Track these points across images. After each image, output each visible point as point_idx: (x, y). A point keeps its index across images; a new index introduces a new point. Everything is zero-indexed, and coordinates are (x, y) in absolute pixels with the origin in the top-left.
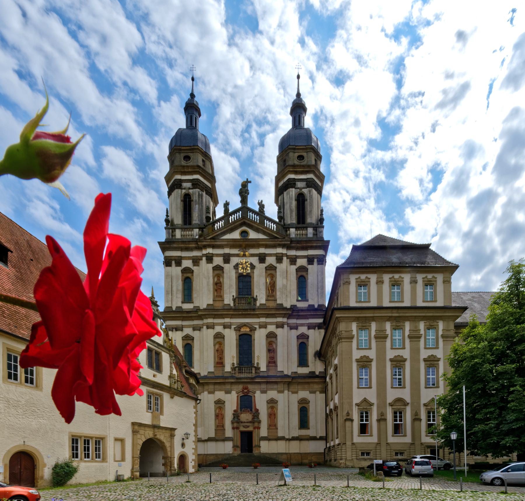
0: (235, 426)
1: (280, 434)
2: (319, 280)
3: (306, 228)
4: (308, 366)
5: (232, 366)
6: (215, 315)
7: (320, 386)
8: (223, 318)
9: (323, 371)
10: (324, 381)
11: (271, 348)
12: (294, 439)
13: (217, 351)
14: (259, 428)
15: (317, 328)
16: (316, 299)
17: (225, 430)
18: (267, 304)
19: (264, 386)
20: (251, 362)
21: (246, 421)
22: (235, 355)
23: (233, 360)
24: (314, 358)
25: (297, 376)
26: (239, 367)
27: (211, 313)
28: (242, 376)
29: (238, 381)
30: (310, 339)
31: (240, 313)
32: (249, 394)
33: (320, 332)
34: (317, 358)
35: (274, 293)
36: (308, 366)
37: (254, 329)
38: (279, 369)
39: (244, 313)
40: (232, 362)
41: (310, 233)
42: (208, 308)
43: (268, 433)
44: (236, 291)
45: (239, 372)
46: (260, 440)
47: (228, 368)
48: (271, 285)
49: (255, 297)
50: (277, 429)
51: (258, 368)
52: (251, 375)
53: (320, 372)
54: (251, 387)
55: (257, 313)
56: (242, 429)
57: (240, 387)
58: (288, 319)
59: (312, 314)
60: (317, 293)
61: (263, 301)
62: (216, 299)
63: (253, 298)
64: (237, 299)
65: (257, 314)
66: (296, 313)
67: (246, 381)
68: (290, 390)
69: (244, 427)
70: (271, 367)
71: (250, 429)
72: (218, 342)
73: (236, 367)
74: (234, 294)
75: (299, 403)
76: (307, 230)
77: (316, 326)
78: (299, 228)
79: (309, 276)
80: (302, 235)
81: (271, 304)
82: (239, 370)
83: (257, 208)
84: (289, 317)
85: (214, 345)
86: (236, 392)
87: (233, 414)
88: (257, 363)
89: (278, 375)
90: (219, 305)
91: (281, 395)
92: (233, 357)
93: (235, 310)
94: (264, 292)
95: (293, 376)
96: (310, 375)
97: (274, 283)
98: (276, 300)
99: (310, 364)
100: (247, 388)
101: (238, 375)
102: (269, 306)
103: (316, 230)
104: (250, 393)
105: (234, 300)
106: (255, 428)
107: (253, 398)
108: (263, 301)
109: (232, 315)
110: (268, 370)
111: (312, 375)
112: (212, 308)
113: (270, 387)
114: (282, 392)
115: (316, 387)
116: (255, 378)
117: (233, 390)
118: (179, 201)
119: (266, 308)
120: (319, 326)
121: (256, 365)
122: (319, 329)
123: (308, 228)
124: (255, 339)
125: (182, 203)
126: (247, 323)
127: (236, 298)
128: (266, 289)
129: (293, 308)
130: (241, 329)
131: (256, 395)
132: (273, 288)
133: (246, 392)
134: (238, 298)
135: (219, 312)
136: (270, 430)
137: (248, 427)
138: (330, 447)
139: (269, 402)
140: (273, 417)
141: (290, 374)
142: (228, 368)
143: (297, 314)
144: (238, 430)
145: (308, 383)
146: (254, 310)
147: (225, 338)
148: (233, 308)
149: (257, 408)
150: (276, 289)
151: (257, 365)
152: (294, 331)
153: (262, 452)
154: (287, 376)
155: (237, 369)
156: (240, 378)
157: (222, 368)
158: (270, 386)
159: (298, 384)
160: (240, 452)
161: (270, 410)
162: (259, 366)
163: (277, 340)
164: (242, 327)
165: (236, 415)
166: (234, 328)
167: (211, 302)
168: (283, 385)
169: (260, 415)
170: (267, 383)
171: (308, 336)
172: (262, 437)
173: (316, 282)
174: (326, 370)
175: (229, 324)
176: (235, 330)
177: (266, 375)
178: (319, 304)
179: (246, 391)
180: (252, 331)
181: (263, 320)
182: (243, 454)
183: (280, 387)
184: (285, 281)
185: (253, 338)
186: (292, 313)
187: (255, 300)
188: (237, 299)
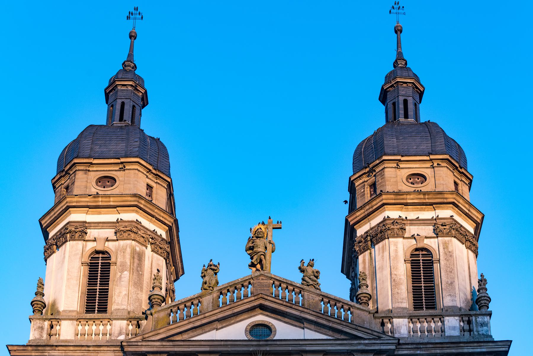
3: (441, 317)
41: (454, 328)
76: (443, 322)
78: (418, 317)
80: (429, 331)
83: (297, 278)
103: (469, 322)
118: (77, 263)
123: (446, 318)
125: (84, 271)
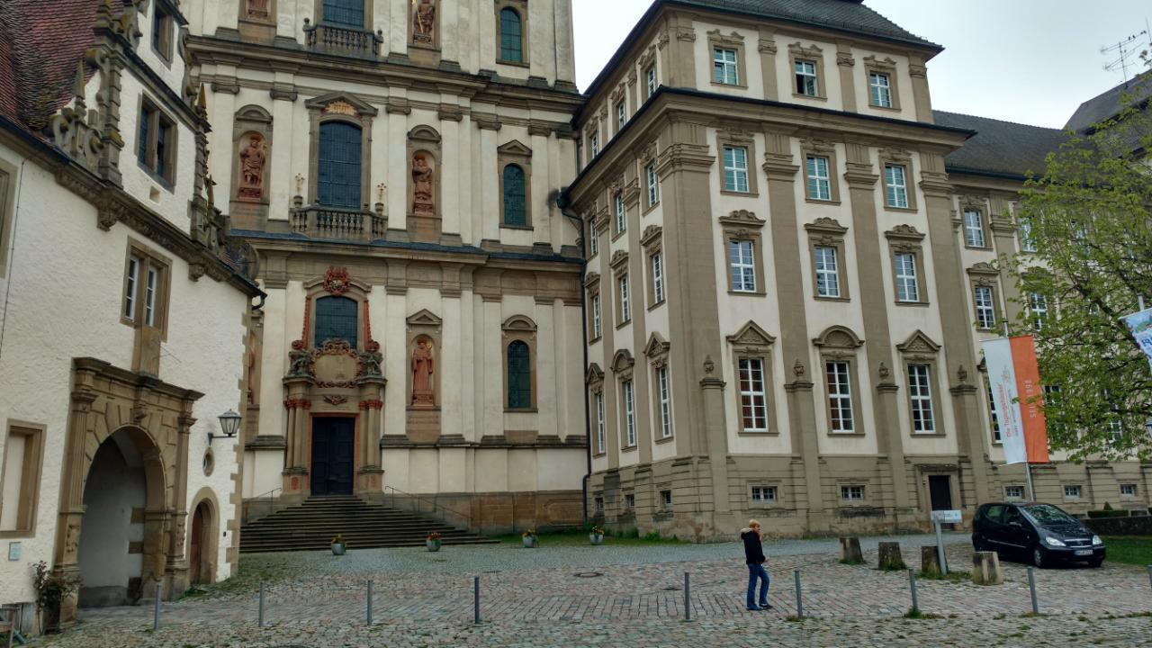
0: (299, 397)
1: (448, 427)
2: (557, 26)
4: (532, 229)
5: (293, 206)
6: (246, 58)
7: (566, 285)
8: (272, 71)
9: (574, 244)
10: (579, 271)
11: (422, 169)
12: (488, 444)
13: (244, 156)
14: (379, 405)
15: (553, 134)
16: (551, 66)
17: (258, 409)
18: (410, 57)
19: (397, 274)
20: (357, 199)
21: (335, 381)
22: (305, 175)
23: (299, 189)
24: (547, 208)
25: (500, 251)
26: (319, 211)
27: (232, 51)
28: (330, 236)
29: (312, 253)
30: (535, 158)
31: (331, 65)
32: (347, 295)
33: (562, 146)
34: (557, 211)
35: (432, 34)
36: (532, 229)
37: (372, 112)
38: (448, 227)
39: (341, 67)
40: (295, 194)
42: (218, 37)
43: (408, 422)
44: (317, 11)
45: (319, 226)
46: (381, 448)
47: (279, 209)
48: (424, 13)
49: (376, 31)
50: (438, 409)
51: (379, 220)
52: (357, 236)
53: (563, 246)
54: (355, 272)
55: (383, 72)
56: (321, 407)
57: (320, 271)
58: (472, 100)
59: (542, 98)
60: (552, 53)
61: (401, 47)
62: (249, 19)
63: (372, 34)
64: (320, 31)
65: (382, 77)
66: (498, 89)
67: (340, 252)
68: (480, 289)
69: (328, 401)
70: (422, 221)
71: (351, 407)
72: (248, 133)
73: (310, 210)
74: (311, 18)
75: (506, 331)
77: (551, 130)
79: (530, 11)
81: (423, 59)
82: (319, 219)
84: (478, 96)
85: (236, 140)
86: (305, 284)
87: (293, 357)
88: (377, 204)
89: (443, 243)
90: (256, 34)
91: (452, 303)
92: (299, 180)
93: (310, 55)
94: (405, 27)
95: (487, 250)
96: (537, 253)
97: (434, 10)
98: (440, 52)
99: (535, 223)
100: (342, 276)
101: (312, 233)
102: (419, 63)
104: (353, 290)
105: (310, 32)
106: (366, 406)
107: (361, 305)
108: (401, 47)
109: (302, 66)
110: (411, 227)
111: (542, 254)
112: (237, 39)
113: (416, 277)
114: (455, 294)
115: (554, 286)
116: (371, 246)
117: (296, 279)
119: (408, 64)
120: (561, 132)
121: (373, 209)
122: (558, 137)
124: (373, 139)
126: (349, 94)
127: (316, 26)
128: (410, 20)
129: (485, 77)
130: (329, 107)
131: (370, 297)
132: (428, 22)
133: (338, 287)
134: (326, 27)
135: (260, 52)
136: (416, 413)
137: (343, 401)
138: (613, 474)
139: (413, 321)
140: (424, 368)
141: (477, 244)
142: (279, 209)
143: (499, 93)
144: (307, 412)
145: (533, 274)
146: (374, 64)
147: (275, 123)
148: (306, 49)
149: (374, 338)
150: (438, 26)
151: (377, 210)
152: (487, 134)
153: (388, 491)
154: (467, 250)
155: (312, 216)
156: (323, 243)
157: (257, 207)
158: (416, 274)
159: (502, 275)
160: (308, 492)
161: (414, 346)
162: (384, 214)
163: (440, 148)
164: (332, 101)
165: (301, 360)
166: (307, 101)
167: (233, 24)
168: (457, 273)
169: (382, 364)
170: (410, 263)
171: (531, 151)
172: (387, 437)
173: (549, 28)
174: (582, 242)
175: (291, 88)
176: (308, 107)
177: (405, 239)
178: (559, 78)
179: (337, 282)
180: (364, 118)
181: (398, 93)
182: (322, 498)
183: (451, 278)
184: (464, 13)
185: (365, 135)
186: (487, 88)
187: (377, 41)
188: (320, 31)
